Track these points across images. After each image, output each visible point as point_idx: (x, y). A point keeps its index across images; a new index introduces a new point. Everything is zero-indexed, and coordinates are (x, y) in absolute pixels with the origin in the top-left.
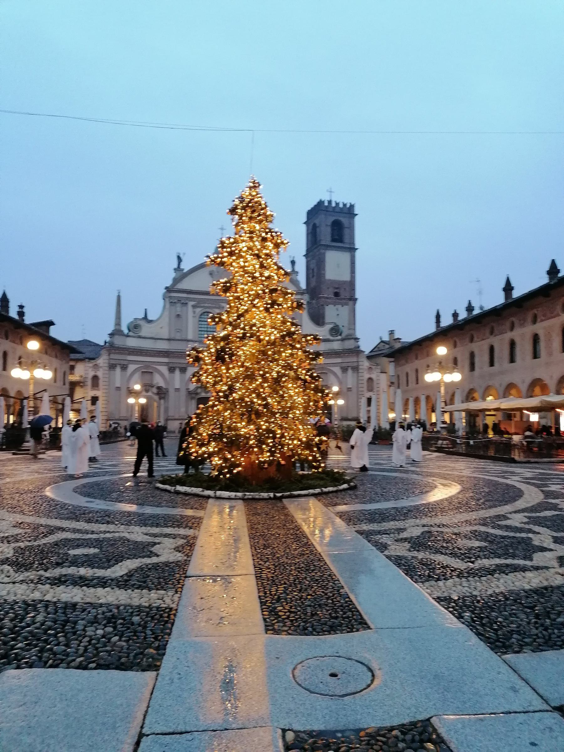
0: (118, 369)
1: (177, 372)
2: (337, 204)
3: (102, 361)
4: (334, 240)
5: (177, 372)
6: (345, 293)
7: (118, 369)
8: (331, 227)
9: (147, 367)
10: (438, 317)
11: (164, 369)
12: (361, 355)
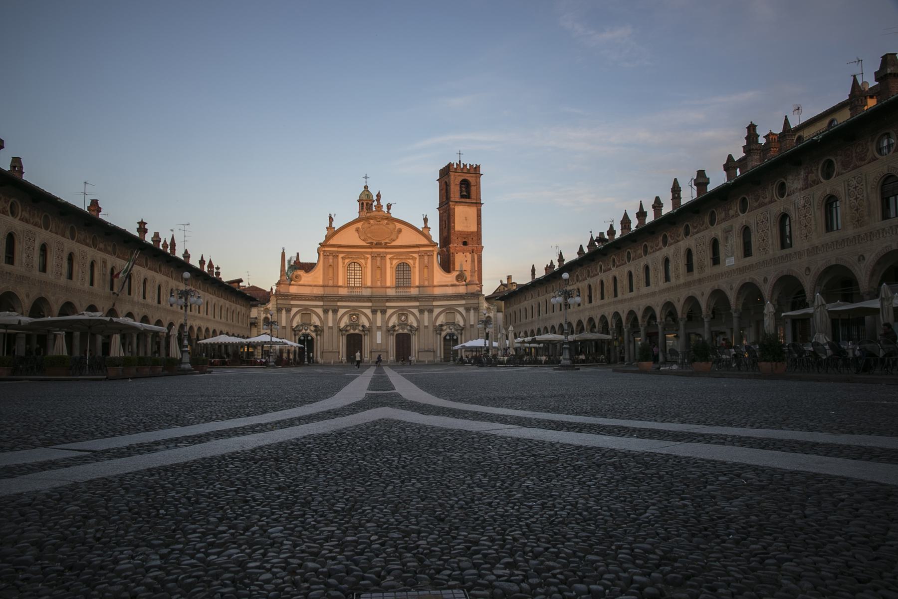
0: (284, 312)
1: (330, 313)
2: (465, 166)
3: (271, 306)
4: (462, 196)
5: (330, 313)
6: (473, 241)
7: (284, 312)
8: (459, 186)
9: (306, 309)
10: (533, 270)
11: (320, 311)
12: (481, 298)
